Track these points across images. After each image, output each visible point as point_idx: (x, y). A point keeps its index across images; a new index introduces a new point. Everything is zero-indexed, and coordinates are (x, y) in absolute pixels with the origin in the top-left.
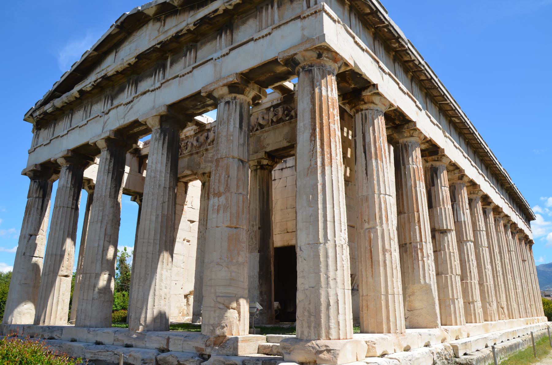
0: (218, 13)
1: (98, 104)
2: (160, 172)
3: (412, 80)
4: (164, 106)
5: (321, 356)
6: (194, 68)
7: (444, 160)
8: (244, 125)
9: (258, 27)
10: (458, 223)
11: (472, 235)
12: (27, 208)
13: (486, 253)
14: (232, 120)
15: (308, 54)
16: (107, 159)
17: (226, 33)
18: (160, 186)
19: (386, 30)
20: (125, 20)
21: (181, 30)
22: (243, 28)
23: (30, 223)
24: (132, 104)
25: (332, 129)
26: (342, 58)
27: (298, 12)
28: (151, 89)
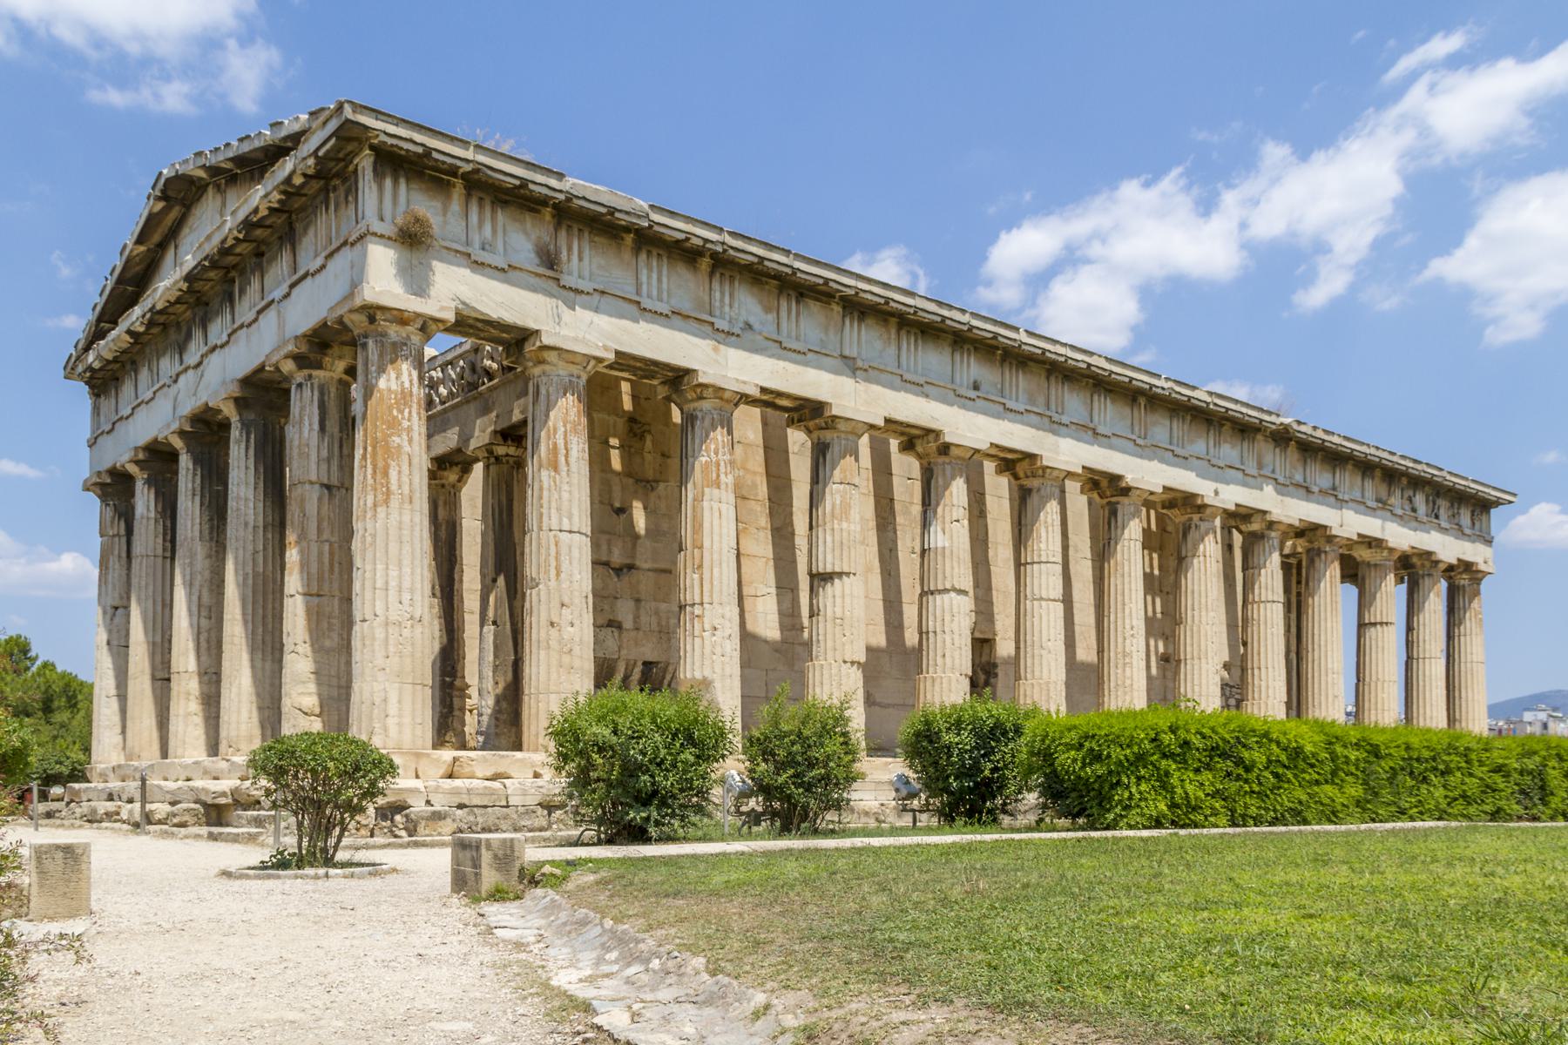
26: (418, 315)
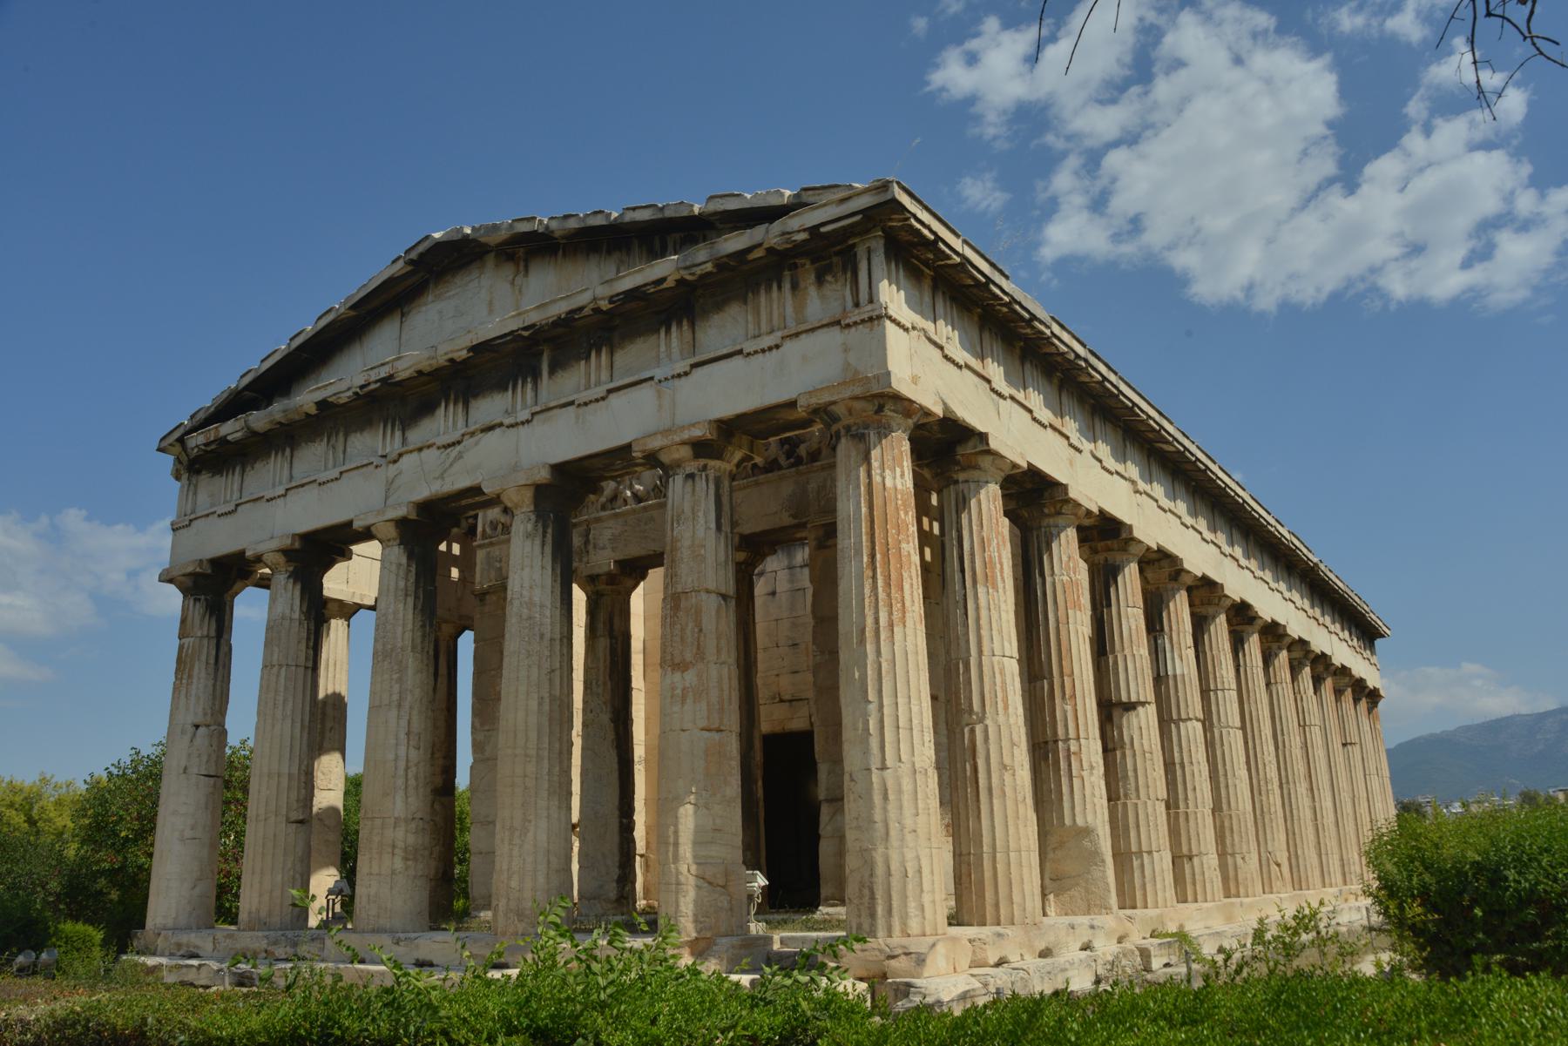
0: (665, 286)
1: (366, 434)
2: (542, 606)
3: (1060, 389)
4: (544, 465)
5: (893, 963)
6: (610, 391)
7: (1134, 549)
8: (725, 521)
9: (751, 326)
10: (1160, 679)
11: (1199, 707)
12: (179, 660)
13: (1234, 741)
14: (701, 514)
15: (858, 405)
16: (399, 565)
17: (680, 324)
18: (542, 636)
19: (1005, 310)
20: (429, 251)
21: (581, 309)
22: (716, 319)
23: (193, 699)
24: (458, 448)
25: (904, 553)
26: (921, 407)
27: (834, 310)
28: (507, 421)
